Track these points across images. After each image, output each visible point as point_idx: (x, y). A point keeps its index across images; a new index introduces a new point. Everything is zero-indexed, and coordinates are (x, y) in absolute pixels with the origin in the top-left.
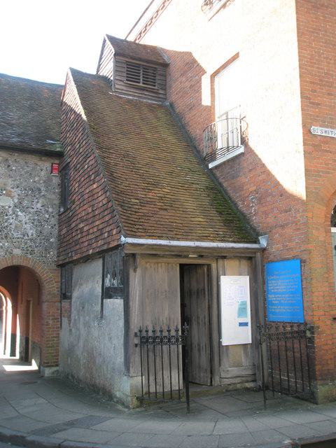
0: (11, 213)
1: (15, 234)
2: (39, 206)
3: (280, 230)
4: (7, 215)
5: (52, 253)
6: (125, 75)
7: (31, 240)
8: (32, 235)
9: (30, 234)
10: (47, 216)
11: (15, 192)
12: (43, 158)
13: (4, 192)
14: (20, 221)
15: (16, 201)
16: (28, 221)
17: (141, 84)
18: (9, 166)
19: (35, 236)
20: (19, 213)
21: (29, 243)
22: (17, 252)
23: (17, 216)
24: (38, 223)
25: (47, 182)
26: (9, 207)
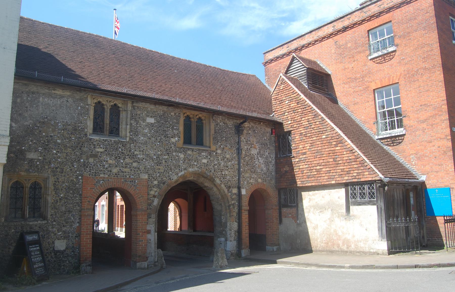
0: (256, 158)
1: (258, 170)
2: (267, 153)
3: (435, 173)
4: (254, 159)
5: (273, 181)
6: (311, 80)
7: (264, 173)
8: (265, 171)
9: (264, 171)
10: (270, 160)
11: (257, 146)
12: (268, 126)
13: (253, 146)
14: (260, 163)
15: (258, 151)
16: (263, 163)
17: (318, 86)
18: (254, 131)
19: (266, 171)
20: (259, 158)
21: (264, 176)
22: (260, 180)
23: (258, 159)
24: (267, 164)
25: (270, 139)
26: (256, 154)
